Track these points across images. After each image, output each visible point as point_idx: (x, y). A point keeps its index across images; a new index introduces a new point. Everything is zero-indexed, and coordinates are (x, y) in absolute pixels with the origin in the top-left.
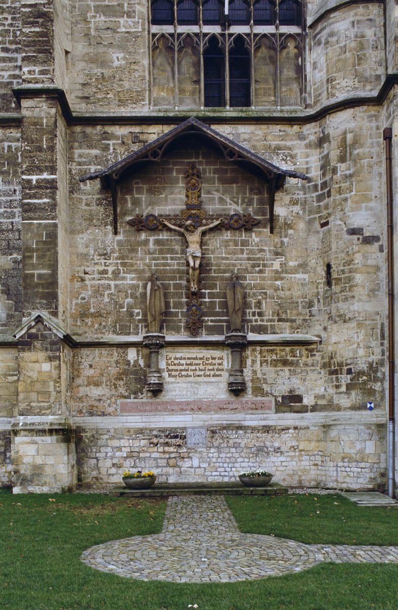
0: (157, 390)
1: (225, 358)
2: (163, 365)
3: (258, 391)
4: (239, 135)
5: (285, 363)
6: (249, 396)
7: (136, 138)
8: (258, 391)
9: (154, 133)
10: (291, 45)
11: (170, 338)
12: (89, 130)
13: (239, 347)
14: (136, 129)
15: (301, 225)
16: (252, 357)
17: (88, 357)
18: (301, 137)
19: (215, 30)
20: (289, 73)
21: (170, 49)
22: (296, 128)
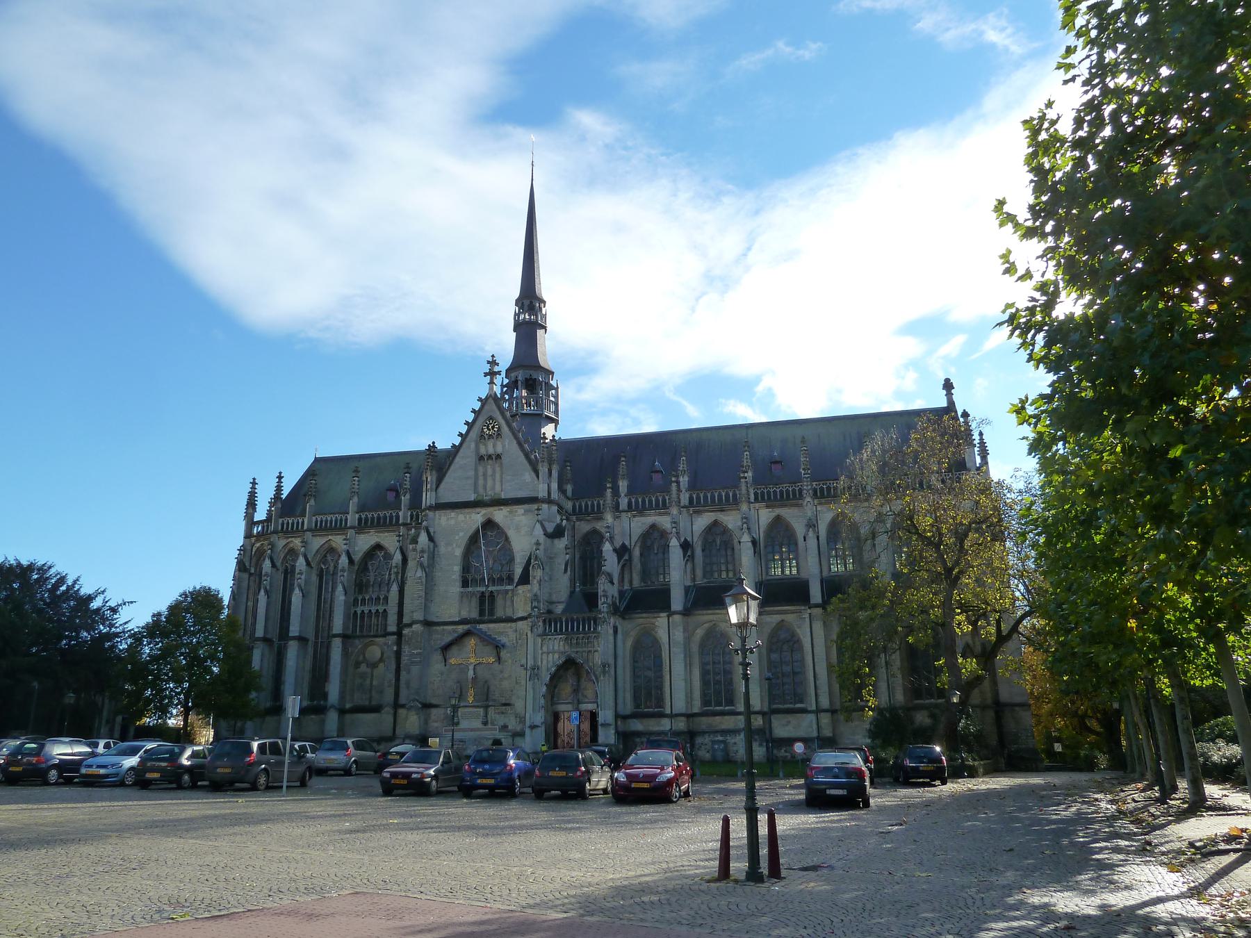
0: (458, 724)
1: (481, 711)
2: (459, 714)
3: (493, 724)
4: (489, 629)
5: (503, 713)
6: (489, 726)
7: (454, 631)
8: (493, 724)
9: (461, 629)
10: (510, 593)
11: (462, 705)
12: (438, 628)
13: (486, 707)
14: (454, 627)
15: (510, 661)
16: (491, 710)
17: (434, 711)
18: (511, 627)
19: (484, 589)
20: (508, 603)
21: (467, 595)
22: (509, 624)
